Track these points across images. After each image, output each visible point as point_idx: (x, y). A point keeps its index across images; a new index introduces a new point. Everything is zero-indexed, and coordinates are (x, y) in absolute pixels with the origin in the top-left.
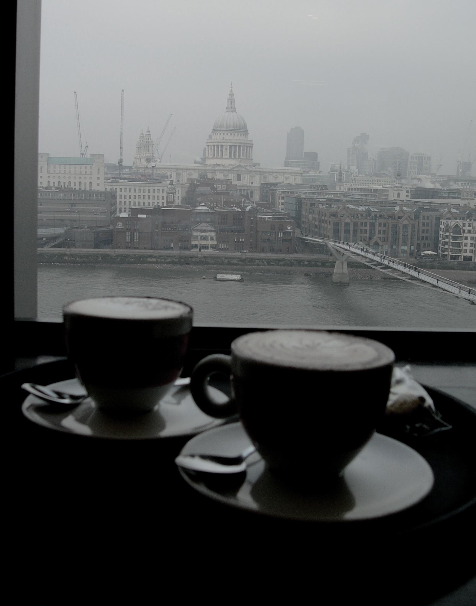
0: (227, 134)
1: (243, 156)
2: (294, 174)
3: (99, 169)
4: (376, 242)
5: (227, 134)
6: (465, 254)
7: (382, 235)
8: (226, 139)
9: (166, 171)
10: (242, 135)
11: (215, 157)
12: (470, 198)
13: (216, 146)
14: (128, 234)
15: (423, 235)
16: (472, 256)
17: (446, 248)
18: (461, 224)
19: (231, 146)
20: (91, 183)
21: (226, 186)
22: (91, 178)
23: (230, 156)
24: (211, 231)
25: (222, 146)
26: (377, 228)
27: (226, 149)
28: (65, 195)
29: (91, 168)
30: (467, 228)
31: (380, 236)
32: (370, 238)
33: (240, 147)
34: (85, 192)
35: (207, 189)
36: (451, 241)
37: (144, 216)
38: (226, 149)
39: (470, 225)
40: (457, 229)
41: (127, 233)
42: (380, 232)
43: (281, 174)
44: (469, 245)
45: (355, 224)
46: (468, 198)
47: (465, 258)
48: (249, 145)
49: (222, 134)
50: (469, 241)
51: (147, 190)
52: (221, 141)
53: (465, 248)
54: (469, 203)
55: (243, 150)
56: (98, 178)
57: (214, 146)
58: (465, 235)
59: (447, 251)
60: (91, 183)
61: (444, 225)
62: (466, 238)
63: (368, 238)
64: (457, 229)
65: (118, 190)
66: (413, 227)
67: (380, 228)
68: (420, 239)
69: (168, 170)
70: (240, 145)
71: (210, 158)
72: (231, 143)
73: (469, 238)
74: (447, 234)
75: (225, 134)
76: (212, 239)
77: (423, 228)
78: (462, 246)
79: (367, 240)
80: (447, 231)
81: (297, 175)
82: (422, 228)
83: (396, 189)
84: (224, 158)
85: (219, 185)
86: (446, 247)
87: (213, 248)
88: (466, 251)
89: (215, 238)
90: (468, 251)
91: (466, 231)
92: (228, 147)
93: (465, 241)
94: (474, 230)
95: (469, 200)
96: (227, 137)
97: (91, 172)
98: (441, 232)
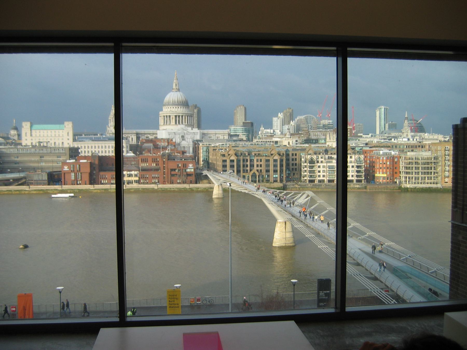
0: (173, 108)
1: (185, 122)
2: (223, 135)
3: (68, 133)
4: (254, 173)
5: (173, 108)
6: (319, 178)
7: (259, 168)
8: (173, 112)
9: (130, 136)
10: (184, 108)
11: (165, 124)
12: (333, 141)
13: (165, 117)
14: (73, 174)
15: (293, 167)
16: (324, 180)
17: (306, 175)
18: (315, 157)
19: (176, 116)
20: (63, 143)
21: (167, 143)
22: (63, 139)
23: (176, 123)
24: (135, 171)
25: (170, 116)
26: (255, 163)
27: (173, 118)
28: (36, 150)
29: (63, 132)
30: (320, 160)
31: (258, 168)
32: (251, 170)
33: (182, 116)
34: (59, 149)
35: (151, 145)
36: (308, 169)
37: (85, 161)
38: (173, 118)
39: (321, 158)
40: (312, 162)
41: (72, 174)
42: (257, 166)
43: (213, 135)
44: (321, 172)
45: (238, 161)
46: (331, 141)
47: (320, 181)
48: (190, 115)
49: (170, 108)
50: (321, 169)
51: (104, 147)
52: (169, 113)
53: (319, 174)
54: (332, 144)
55: (185, 118)
56: (68, 139)
57: (164, 116)
58: (318, 164)
59: (306, 177)
60: (63, 143)
61: (304, 158)
62: (319, 167)
63: (249, 170)
64: (312, 162)
65: (83, 147)
66: (281, 161)
67: (258, 163)
68: (291, 170)
69: (131, 134)
70: (182, 115)
71: (162, 125)
72: (176, 113)
73: (321, 167)
74: (306, 164)
75: (172, 108)
76: (136, 176)
77: (293, 162)
78: (317, 172)
79: (249, 171)
80: (306, 162)
81: (225, 135)
82: (291, 162)
83: (287, 139)
84: (172, 125)
85: (162, 142)
86: (305, 174)
87: (136, 182)
88: (319, 176)
89: (138, 175)
90: (321, 176)
91: (320, 162)
92: (174, 117)
93: (319, 169)
94: (325, 161)
95: (332, 142)
96: (174, 110)
97: (63, 135)
98: (302, 164)
